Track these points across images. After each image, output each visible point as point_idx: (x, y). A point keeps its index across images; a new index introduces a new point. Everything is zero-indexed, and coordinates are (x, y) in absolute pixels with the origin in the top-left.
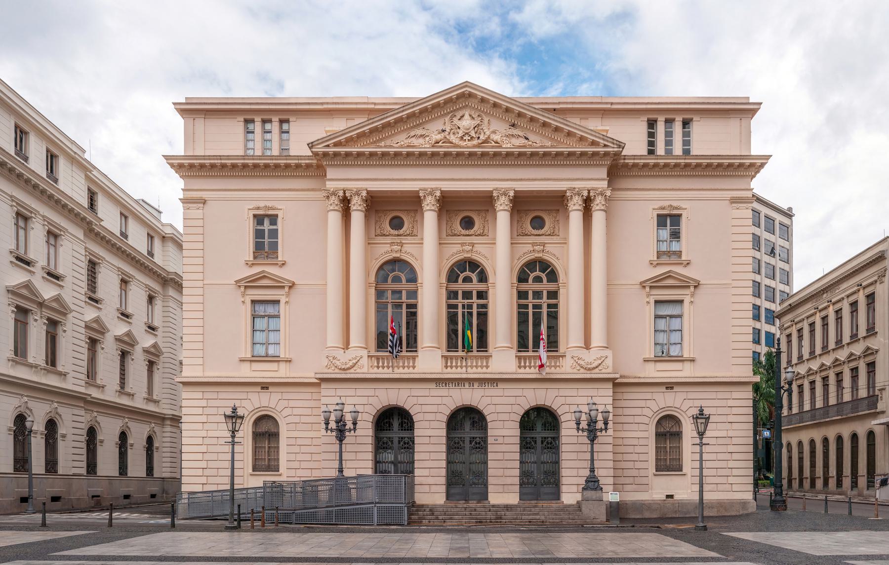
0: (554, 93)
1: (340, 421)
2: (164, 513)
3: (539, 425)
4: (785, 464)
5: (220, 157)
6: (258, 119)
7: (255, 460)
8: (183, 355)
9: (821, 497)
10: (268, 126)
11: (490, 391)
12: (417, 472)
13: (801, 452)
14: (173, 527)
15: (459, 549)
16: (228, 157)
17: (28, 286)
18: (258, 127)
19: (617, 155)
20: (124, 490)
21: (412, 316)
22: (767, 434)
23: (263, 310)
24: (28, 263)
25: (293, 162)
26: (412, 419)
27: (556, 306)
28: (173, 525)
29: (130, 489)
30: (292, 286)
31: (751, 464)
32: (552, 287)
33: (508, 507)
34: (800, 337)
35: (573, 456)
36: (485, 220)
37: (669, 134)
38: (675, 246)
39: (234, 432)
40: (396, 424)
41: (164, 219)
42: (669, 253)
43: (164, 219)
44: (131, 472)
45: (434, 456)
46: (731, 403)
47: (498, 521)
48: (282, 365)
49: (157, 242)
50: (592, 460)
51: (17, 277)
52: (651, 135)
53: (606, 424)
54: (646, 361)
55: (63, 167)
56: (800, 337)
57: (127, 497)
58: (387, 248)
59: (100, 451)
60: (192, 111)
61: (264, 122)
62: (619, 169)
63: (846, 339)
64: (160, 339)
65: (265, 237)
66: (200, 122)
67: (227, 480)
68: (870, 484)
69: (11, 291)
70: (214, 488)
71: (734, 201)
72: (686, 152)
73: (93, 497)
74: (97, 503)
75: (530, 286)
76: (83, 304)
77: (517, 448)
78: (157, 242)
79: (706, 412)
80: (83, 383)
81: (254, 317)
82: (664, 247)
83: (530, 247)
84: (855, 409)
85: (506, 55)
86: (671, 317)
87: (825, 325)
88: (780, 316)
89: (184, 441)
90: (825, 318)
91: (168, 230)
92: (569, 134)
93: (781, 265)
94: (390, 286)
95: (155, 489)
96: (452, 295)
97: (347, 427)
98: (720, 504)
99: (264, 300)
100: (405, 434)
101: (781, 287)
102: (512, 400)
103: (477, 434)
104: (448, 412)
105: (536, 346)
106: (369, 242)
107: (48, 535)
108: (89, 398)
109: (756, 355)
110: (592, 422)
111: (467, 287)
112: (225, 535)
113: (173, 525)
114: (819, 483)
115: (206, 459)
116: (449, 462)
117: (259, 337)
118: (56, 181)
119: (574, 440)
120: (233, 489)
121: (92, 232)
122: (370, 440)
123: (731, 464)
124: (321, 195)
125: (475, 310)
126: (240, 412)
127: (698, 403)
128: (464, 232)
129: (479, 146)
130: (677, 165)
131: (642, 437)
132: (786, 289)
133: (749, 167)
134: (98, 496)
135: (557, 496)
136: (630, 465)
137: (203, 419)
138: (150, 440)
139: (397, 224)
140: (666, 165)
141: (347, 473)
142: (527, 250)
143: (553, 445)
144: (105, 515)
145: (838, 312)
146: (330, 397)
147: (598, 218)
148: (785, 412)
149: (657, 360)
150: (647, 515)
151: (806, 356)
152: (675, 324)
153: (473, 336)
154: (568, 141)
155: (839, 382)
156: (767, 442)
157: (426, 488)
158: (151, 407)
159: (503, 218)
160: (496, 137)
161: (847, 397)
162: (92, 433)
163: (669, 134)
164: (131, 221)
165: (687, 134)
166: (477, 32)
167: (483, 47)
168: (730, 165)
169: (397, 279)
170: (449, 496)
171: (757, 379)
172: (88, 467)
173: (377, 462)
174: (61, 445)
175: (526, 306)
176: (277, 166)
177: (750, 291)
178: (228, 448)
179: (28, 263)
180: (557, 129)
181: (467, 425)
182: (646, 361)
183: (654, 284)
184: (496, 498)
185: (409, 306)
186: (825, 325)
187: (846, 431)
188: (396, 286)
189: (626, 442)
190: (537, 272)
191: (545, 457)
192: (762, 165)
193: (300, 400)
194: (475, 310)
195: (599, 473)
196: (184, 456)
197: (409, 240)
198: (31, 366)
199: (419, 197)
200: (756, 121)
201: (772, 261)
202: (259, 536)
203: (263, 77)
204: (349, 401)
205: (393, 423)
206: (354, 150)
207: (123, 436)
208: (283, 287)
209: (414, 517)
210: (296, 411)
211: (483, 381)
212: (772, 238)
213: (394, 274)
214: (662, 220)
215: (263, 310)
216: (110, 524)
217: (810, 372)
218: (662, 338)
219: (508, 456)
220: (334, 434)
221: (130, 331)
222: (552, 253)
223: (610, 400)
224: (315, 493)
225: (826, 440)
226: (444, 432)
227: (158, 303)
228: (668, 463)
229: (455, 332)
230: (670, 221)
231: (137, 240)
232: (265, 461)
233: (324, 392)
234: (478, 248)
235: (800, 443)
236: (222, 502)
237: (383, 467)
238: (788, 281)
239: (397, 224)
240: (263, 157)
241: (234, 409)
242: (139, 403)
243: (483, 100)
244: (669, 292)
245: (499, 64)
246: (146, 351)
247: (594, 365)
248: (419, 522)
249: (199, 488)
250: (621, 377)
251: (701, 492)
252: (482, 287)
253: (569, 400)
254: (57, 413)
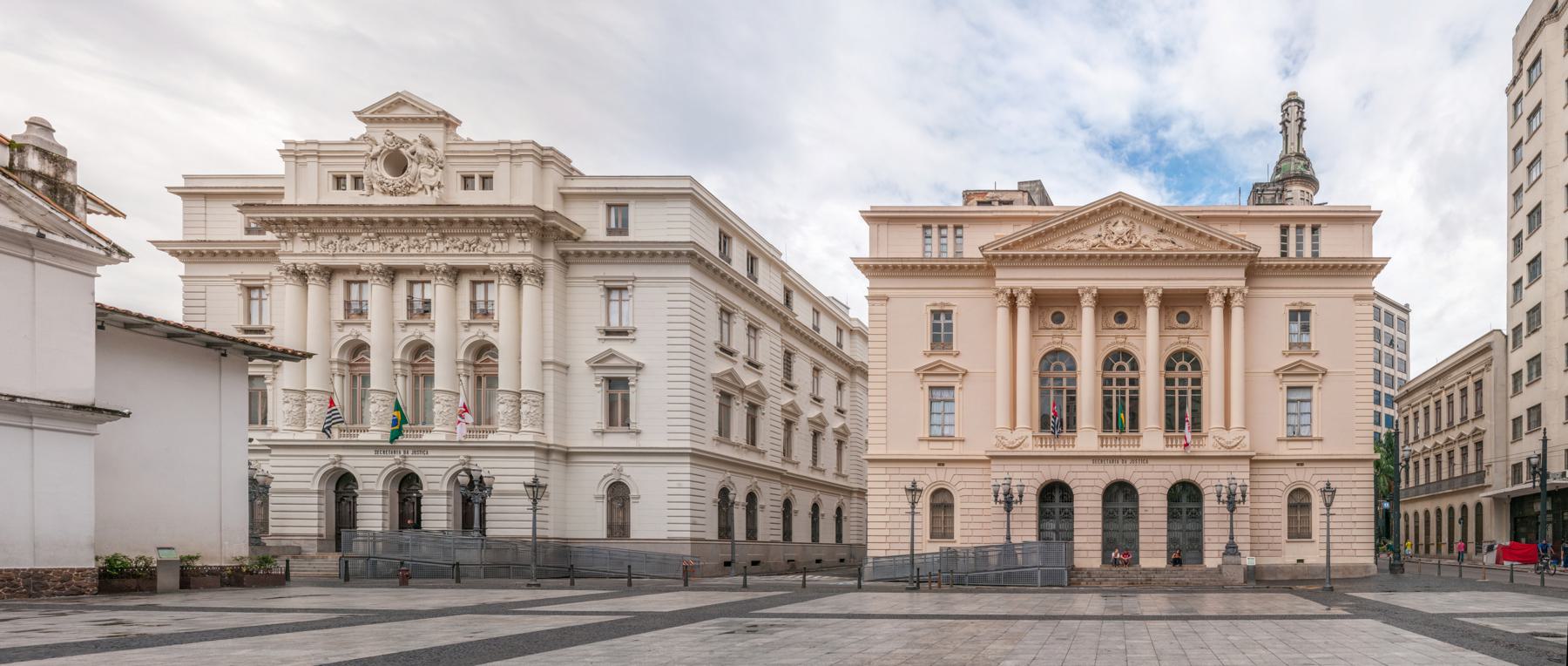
0: (1198, 202)
1: (1008, 493)
2: (852, 576)
3: (1184, 497)
4: (1402, 532)
5: (901, 259)
6: (935, 225)
7: (933, 528)
8: (868, 435)
9: (1435, 561)
10: (944, 232)
11: (1141, 467)
12: (1076, 539)
13: (1417, 522)
14: (859, 588)
15: (1114, 608)
16: (909, 259)
17: (731, 373)
18: (935, 232)
19: (1254, 257)
20: (817, 556)
21: (1072, 400)
22: (1386, 505)
23: (940, 395)
24: (731, 353)
25: (966, 263)
27: (1199, 391)
28: (860, 586)
29: (821, 555)
30: (965, 373)
31: (1372, 532)
32: (1196, 374)
33: (1157, 571)
34: (1416, 419)
35: (1215, 525)
36: (1137, 315)
37: (1299, 239)
38: (1305, 339)
39: (913, 503)
40: (1057, 496)
41: (852, 314)
42: (1300, 345)
43: (852, 314)
44: (822, 540)
45: (1091, 525)
46: (1354, 478)
47: (1149, 582)
48: (957, 444)
49: (845, 335)
51: (721, 366)
52: (1284, 239)
54: (1279, 440)
55: (762, 268)
56: (1416, 419)
57: (818, 561)
58: (1050, 340)
59: (795, 521)
60: (876, 218)
61: (940, 228)
62: (1255, 269)
63: (1457, 421)
64: (848, 421)
65: (941, 329)
66: (883, 228)
67: (908, 546)
68: (1478, 550)
69: (715, 379)
70: (896, 553)
71: (1358, 298)
72: (1315, 255)
74: (792, 567)
75: (1177, 374)
77: (1165, 518)
78: (845, 335)
79: (1333, 485)
81: (931, 402)
82: (1295, 339)
83: (1176, 340)
84: (1465, 483)
85: (1155, 169)
87: (1438, 409)
88: (1398, 401)
89: (870, 511)
90: (1438, 403)
91: (855, 324)
92: (1211, 239)
93: (1399, 355)
94: (1052, 374)
95: (843, 554)
96: (1107, 381)
98: (1346, 568)
99: (940, 386)
100: (1066, 506)
101: (1399, 375)
102: (1161, 475)
103: (1129, 505)
104: (1104, 486)
105: (1182, 427)
106: (1034, 335)
107: (749, 595)
109: (1377, 435)
110: (1231, 495)
111: (1121, 374)
112: (906, 595)
113: (860, 586)
114: (1433, 549)
115: (889, 527)
117: (936, 419)
118: (756, 280)
120: (912, 555)
121: (788, 326)
122: (1034, 511)
123: (1355, 532)
124: (991, 292)
125: (1127, 395)
126: (919, 486)
127: (1326, 478)
129: (1131, 249)
130: (1306, 266)
131: (1276, 509)
132: (1404, 376)
133: (1369, 268)
136: (1265, 533)
137: (887, 492)
138: (839, 510)
139: (1058, 318)
140: (1297, 266)
141: (1014, 540)
142: (1174, 342)
143: (1197, 515)
144: (800, 577)
145: (1450, 397)
146: (999, 473)
147: (1237, 313)
148: (1403, 486)
149: (1289, 439)
150: (1280, 577)
151: (1421, 436)
152: (1305, 407)
153: (1126, 418)
154: (1210, 245)
155: (1451, 459)
156: (1387, 512)
157: (1084, 554)
158: (840, 482)
159: (1152, 313)
160: (1146, 241)
161: (1458, 473)
162: (787, 504)
163: (1299, 239)
164: (823, 317)
165: (1315, 239)
166: (1129, 148)
167: (1134, 162)
168: (1354, 267)
169: (1058, 368)
170: (1105, 559)
171: (1378, 456)
173: (1040, 530)
174: (760, 515)
175: (1173, 392)
176: (952, 267)
177: (1372, 378)
178: (909, 518)
179: (731, 353)
180: (1200, 234)
181: (1121, 497)
182: (1279, 440)
183: (1287, 372)
184: (1146, 562)
185: (1069, 392)
186: (1438, 409)
187: (1457, 503)
188: (1058, 374)
190: (1183, 361)
191: (1190, 526)
192: (1383, 266)
193: (973, 475)
194: (1127, 395)
195: (1237, 540)
196: (870, 525)
197: (1069, 332)
198: (733, 445)
200: (1377, 228)
201: (1391, 352)
202: (936, 596)
203: (939, 188)
204: (1016, 475)
205: (1055, 496)
206: (1020, 253)
207: (815, 507)
209: (1073, 579)
210: (969, 485)
211: (1134, 459)
212: (1391, 331)
213: (1056, 363)
214: (1293, 315)
215: (940, 395)
216: (804, 585)
217: (1425, 451)
218: (1294, 420)
219: (1157, 525)
222: (1196, 344)
223: (1247, 475)
224: (986, 557)
225: (1439, 511)
226: (1100, 504)
227: (847, 388)
228: (1299, 532)
229: (1110, 414)
230: (1300, 316)
231: (828, 333)
232: (941, 529)
233: (994, 468)
234: (1129, 340)
235: (1416, 514)
236: (903, 566)
237: (1046, 534)
238: (1405, 371)
239: (1058, 318)
240: (939, 259)
241: (914, 484)
242: (829, 478)
243: (1135, 209)
244: (1300, 379)
245: (1149, 176)
246: (835, 431)
248: (1078, 584)
249: (882, 554)
251: (1328, 557)
252: (1133, 374)
253: (1211, 475)
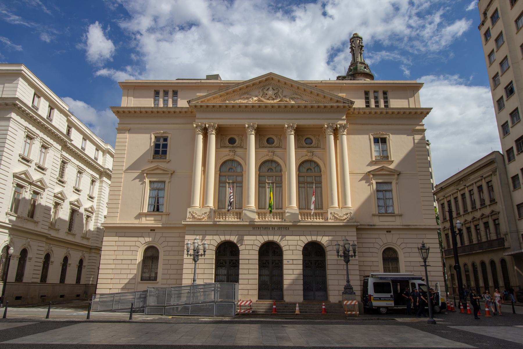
13: (467, 271)
26: (238, 249)
50: (348, 275)
53: (355, 252)
57: (62, 296)
73: (42, 296)
76: (55, 184)
80: (47, 228)
86: (386, 191)
97: (200, 253)
108: (49, 236)
116: (260, 275)
119: (335, 262)
128: (268, 145)
134: (45, 296)
135: (326, 297)
138: (81, 262)
149: (380, 215)
152: (388, 195)
162: (48, 257)
170: (260, 298)
172: (42, 278)
182: (374, 215)
189: (366, 264)
192: (428, 113)
199: (245, 127)
207: (66, 259)
208: (168, 174)
220: (192, 257)
221: (79, 199)
223: (355, 238)
226: (257, 257)
247: (344, 218)
249: (107, 292)
250: (361, 225)
254: (29, 245)
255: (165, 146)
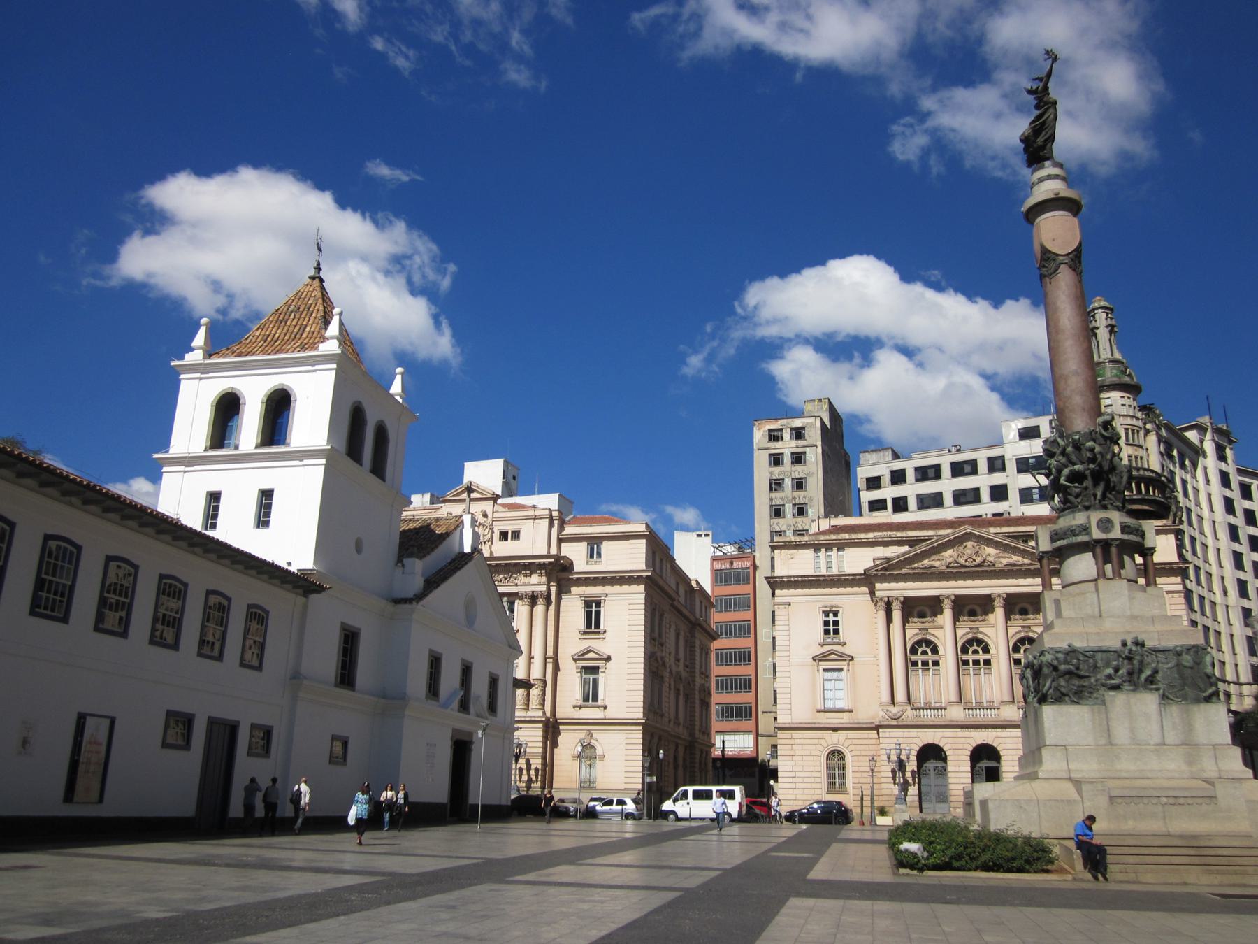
11: (999, 732)
255: (836, 623)
